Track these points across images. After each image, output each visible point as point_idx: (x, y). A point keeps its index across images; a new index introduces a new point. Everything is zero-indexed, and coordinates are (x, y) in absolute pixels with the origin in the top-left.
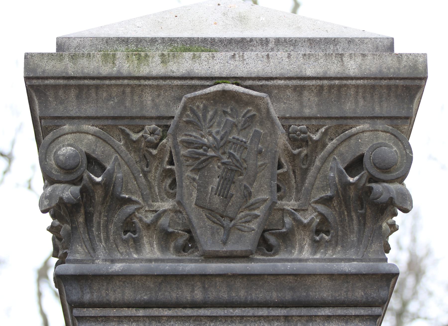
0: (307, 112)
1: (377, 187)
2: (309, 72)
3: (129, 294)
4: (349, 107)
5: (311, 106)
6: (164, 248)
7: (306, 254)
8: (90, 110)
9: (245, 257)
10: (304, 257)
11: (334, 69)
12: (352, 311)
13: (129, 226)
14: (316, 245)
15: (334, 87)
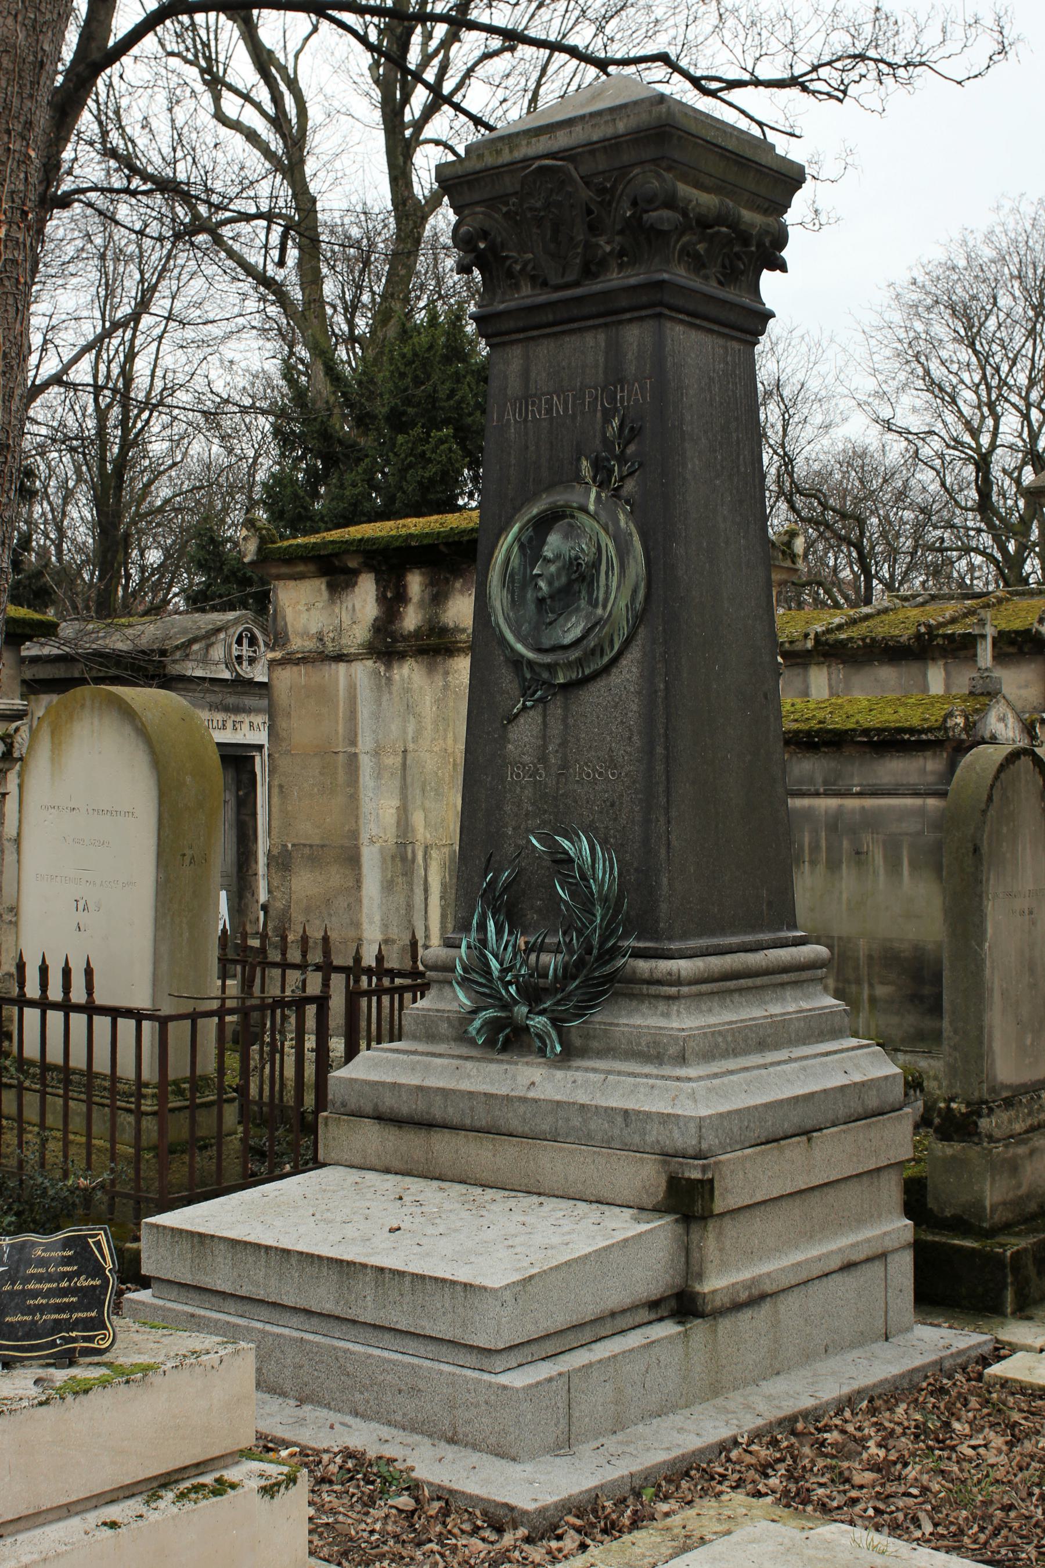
0: (601, 168)
1: (645, 216)
2: (595, 138)
3: (512, 324)
4: (626, 158)
5: (602, 163)
6: (533, 287)
7: (615, 276)
8: (477, 196)
9: (577, 284)
10: (615, 279)
11: (609, 131)
12: (644, 313)
13: (510, 274)
14: (621, 267)
15: (612, 145)
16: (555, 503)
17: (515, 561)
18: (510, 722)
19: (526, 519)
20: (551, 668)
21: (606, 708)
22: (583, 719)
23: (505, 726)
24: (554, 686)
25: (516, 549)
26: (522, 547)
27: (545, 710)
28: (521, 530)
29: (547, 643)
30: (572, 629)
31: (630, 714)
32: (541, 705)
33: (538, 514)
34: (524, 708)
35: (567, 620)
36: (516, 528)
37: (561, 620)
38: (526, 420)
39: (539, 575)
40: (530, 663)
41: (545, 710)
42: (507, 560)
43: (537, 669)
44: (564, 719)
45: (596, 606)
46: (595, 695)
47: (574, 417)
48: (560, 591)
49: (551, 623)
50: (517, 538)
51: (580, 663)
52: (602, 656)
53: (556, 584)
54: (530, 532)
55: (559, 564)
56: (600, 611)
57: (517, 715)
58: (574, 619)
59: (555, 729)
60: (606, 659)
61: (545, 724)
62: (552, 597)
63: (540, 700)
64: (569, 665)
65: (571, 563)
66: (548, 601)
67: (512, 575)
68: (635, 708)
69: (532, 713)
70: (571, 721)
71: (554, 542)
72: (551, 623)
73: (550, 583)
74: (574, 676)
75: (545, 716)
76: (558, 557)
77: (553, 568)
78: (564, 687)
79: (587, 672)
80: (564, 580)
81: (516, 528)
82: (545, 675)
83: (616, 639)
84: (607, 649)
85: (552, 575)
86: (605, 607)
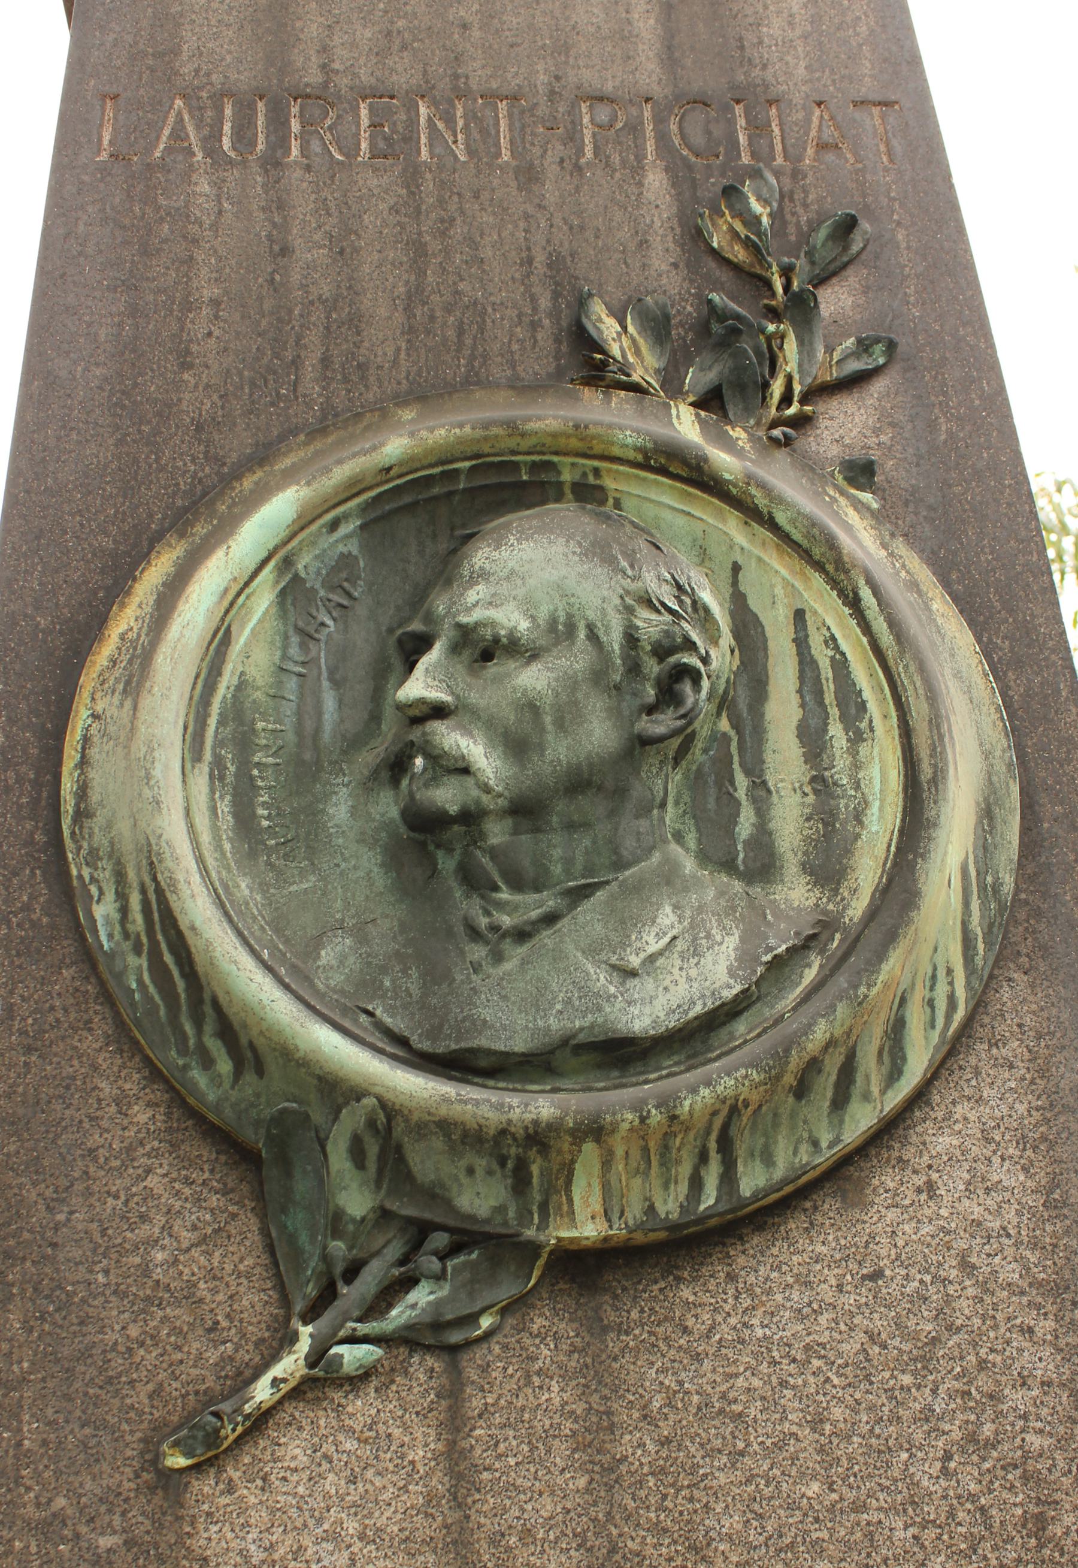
16: (511, 426)
17: (254, 654)
18: (212, 1455)
19: (341, 473)
20: (528, 1159)
21: (863, 1372)
22: (717, 1432)
23: (170, 1483)
24: (533, 1249)
25: (263, 599)
26: (293, 594)
27: (453, 1394)
28: (302, 523)
29: (510, 1028)
30: (675, 955)
31: (1018, 1399)
32: (423, 1371)
33: (409, 464)
34: (321, 1381)
35: (625, 924)
36: (279, 509)
37: (589, 911)
38: (273, 162)
39: (439, 711)
40: (388, 1137)
41: (453, 1394)
42: (220, 640)
43: (426, 1161)
44: (595, 1435)
45: (762, 866)
46: (784, 1301)
47: (528, 175)
48: (579, 782)
49: (522, 935)
50: (281, 556)
51: (724, 1135)
52: (840, 1102)
53: (559, 752)
54: (345, 540)
55: (577, 660)
56: (796, 893)
57: (262, 1419)
58: (667, 917)
59: (535, 1490)
60: (862, 1119)
61: (455, 1459)
62: (525, 810)
63: (434, 1338)
64: (658, 1147)
65: (634, 669)
66: (497, 833)
67: (237, 713)
68: (1043, 1363)
69: (361, 1407)
70: (636, 1447)
71: (524, 573)
72: (522, 935)
73: (516, 746)
74: (669, 1205)
75: (454, 1422)
76: (561, 631)
77: (534, 678)
78: (584, 1269)
79: (752, 1180)
80: (598, 733)
81: (279, 509)
82: (480, 1198)
83: (915, 1017)
84: (869, 1063)
85: (531, 707)
86: (828, 867)
